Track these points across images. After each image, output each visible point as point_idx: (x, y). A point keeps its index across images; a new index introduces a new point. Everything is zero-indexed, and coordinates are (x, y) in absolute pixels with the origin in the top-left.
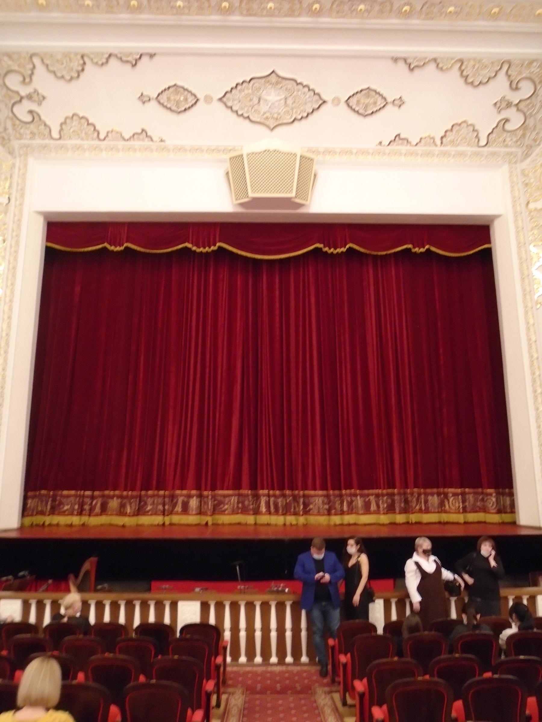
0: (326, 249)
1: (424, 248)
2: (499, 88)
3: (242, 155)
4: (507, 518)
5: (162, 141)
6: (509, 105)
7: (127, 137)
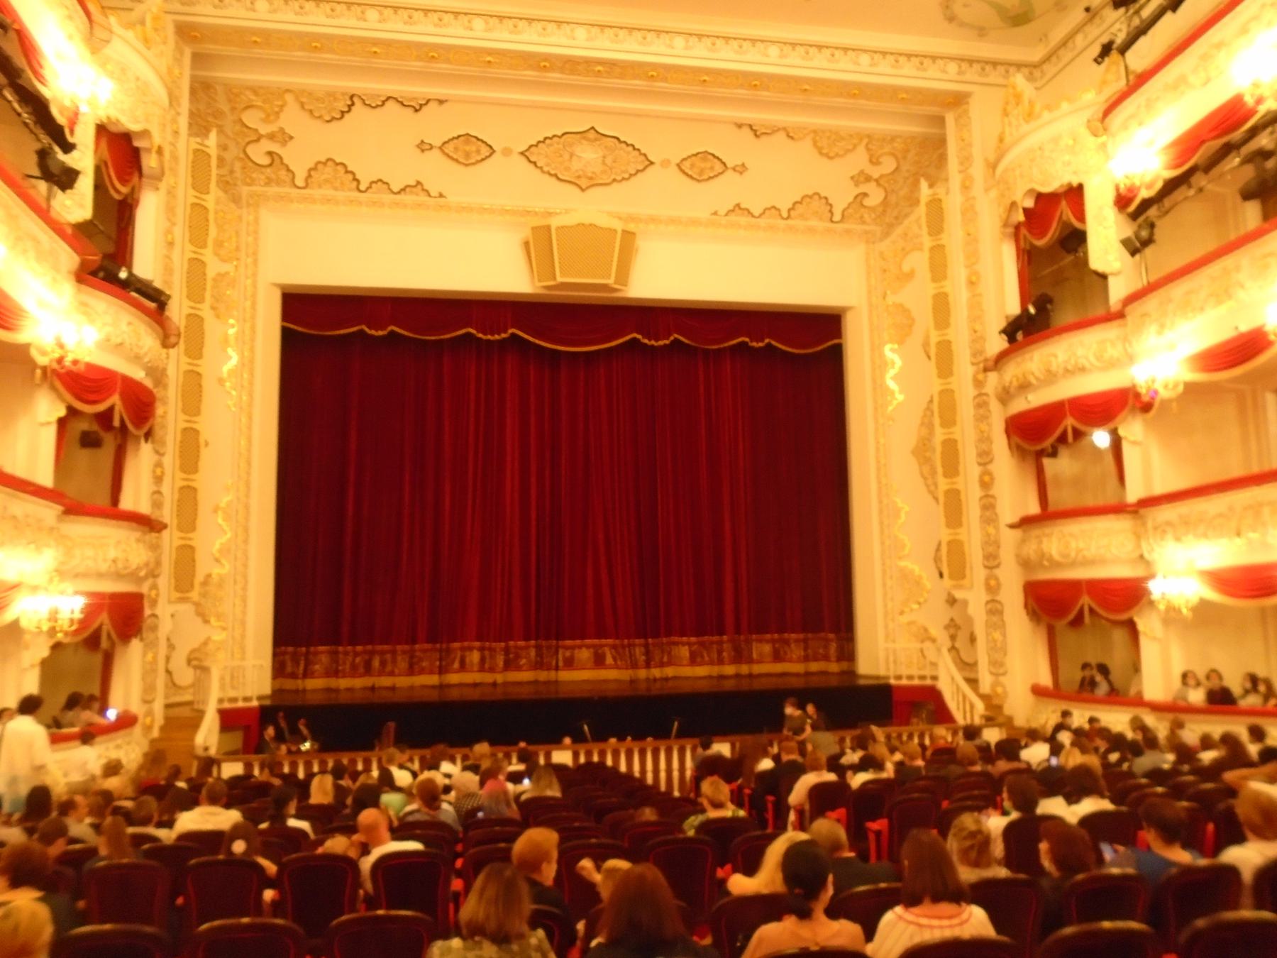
0: (646, 341)
1: (762, 340)
2: (859, 161)
3: (548, 228)
5: (441, 195)
6: (868, 179)
7: (396, 190)
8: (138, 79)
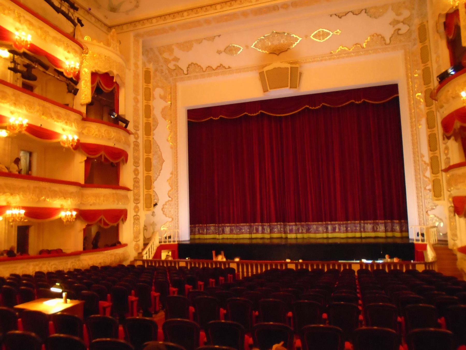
0: (311, 108)
4: (404, 234)
5: (229, 67)
6: (398, 22)
8: (106, 56)
